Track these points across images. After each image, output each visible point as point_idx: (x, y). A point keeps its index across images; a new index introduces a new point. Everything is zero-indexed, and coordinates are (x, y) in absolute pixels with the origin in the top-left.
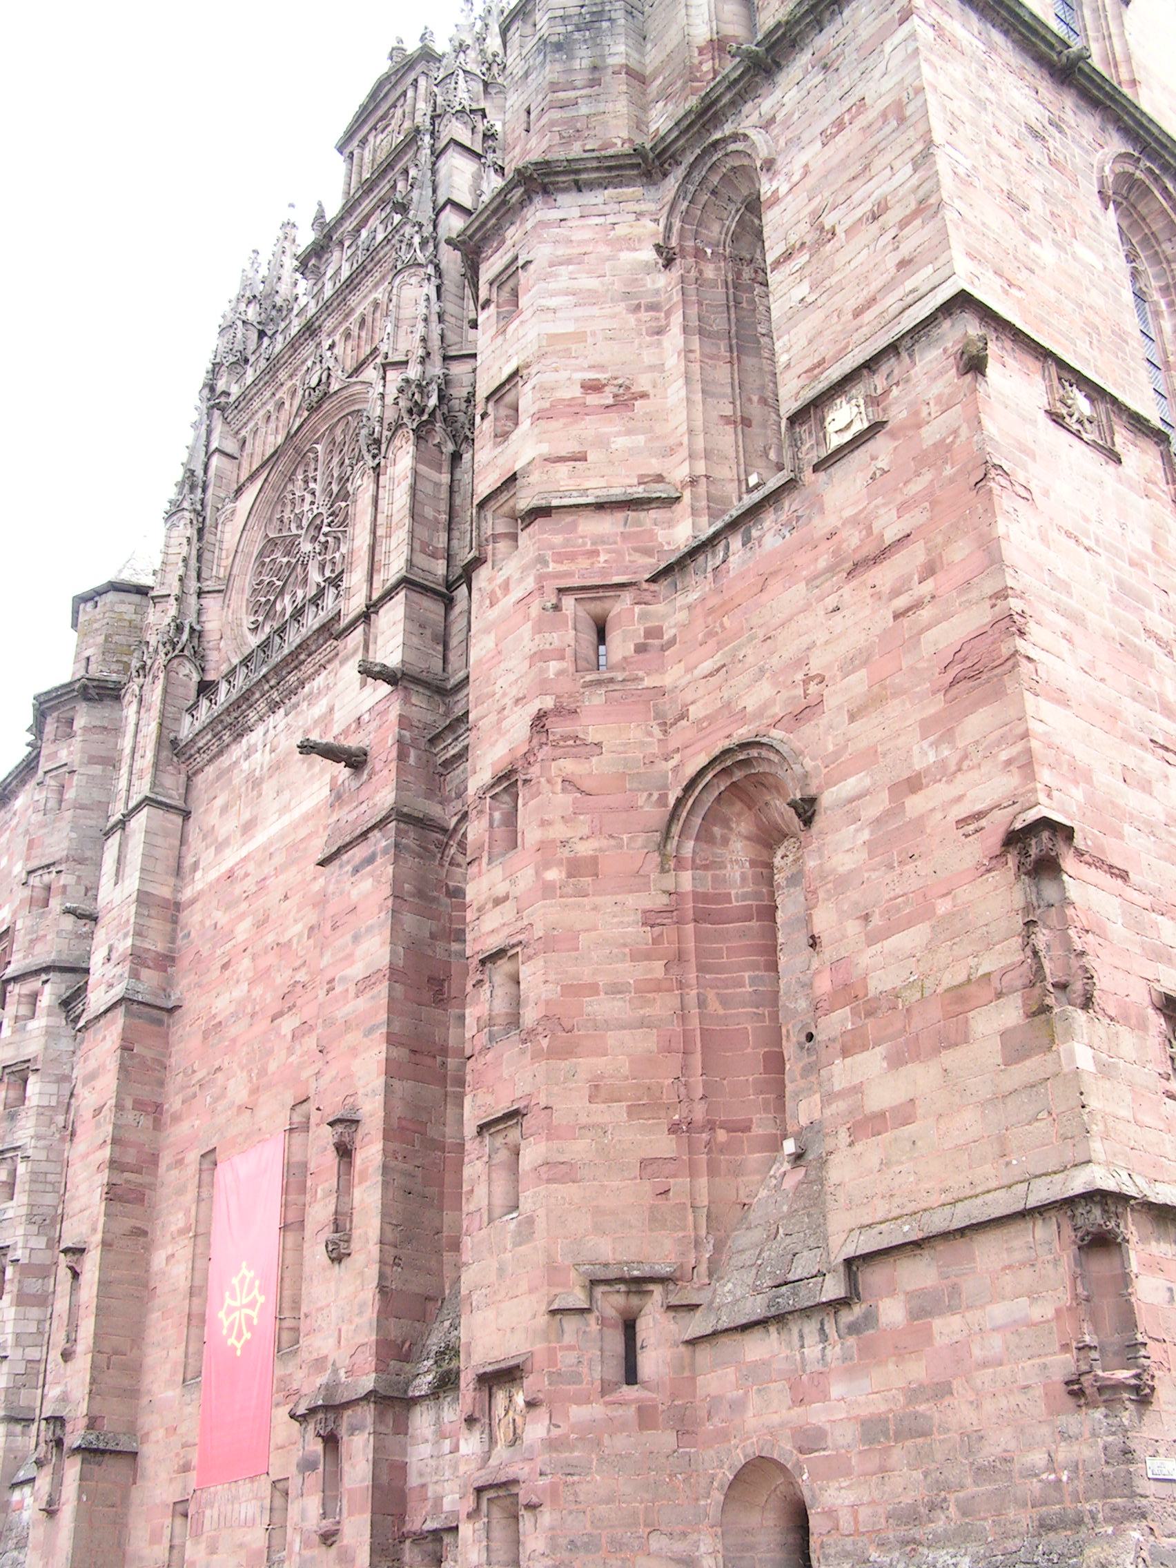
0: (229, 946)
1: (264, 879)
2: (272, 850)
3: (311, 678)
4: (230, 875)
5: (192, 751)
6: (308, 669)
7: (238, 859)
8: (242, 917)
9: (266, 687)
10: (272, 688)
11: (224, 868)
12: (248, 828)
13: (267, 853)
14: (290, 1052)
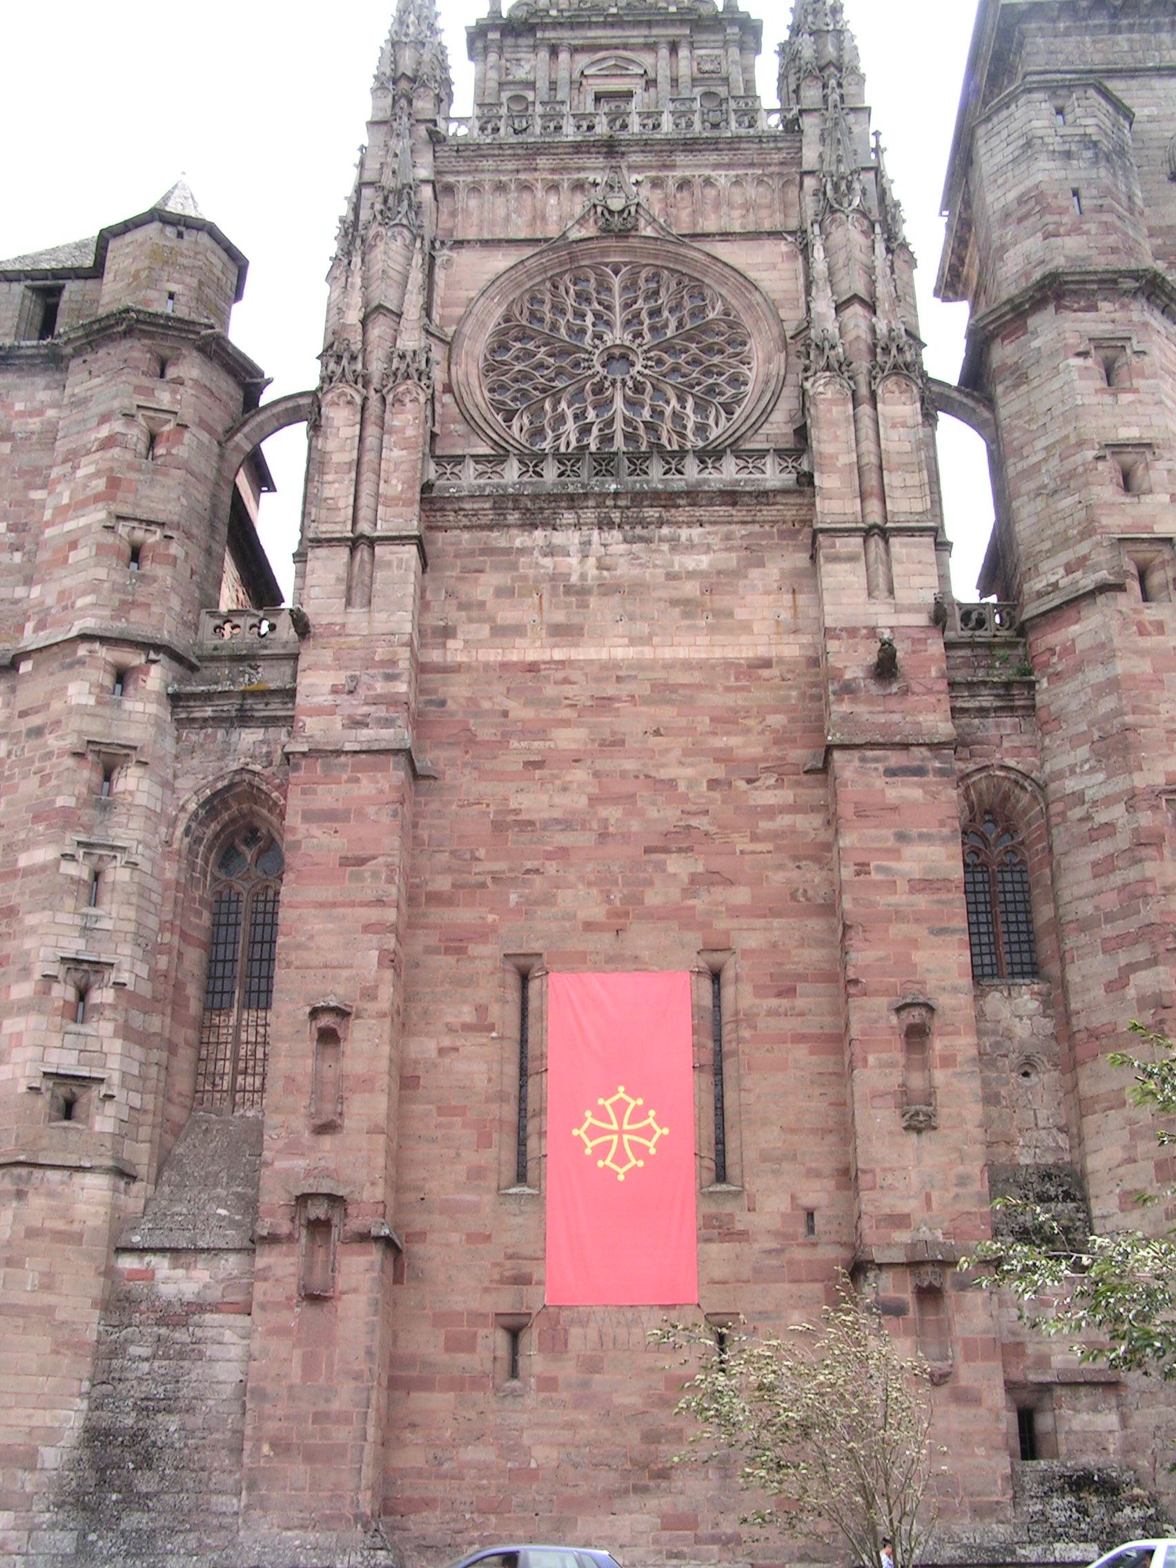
0: (536, 744)
1: (609, 699)
2: (620, 673)
3: (678, 524)
4: (533, 668)
5: (449, 507)
6: (680, 515)
7: (547, 657)
8: (566, 723)
9: (610, 502)
10: (616, 507)
11: (514, 657)
12: (561, 632)
13: (612, 671)
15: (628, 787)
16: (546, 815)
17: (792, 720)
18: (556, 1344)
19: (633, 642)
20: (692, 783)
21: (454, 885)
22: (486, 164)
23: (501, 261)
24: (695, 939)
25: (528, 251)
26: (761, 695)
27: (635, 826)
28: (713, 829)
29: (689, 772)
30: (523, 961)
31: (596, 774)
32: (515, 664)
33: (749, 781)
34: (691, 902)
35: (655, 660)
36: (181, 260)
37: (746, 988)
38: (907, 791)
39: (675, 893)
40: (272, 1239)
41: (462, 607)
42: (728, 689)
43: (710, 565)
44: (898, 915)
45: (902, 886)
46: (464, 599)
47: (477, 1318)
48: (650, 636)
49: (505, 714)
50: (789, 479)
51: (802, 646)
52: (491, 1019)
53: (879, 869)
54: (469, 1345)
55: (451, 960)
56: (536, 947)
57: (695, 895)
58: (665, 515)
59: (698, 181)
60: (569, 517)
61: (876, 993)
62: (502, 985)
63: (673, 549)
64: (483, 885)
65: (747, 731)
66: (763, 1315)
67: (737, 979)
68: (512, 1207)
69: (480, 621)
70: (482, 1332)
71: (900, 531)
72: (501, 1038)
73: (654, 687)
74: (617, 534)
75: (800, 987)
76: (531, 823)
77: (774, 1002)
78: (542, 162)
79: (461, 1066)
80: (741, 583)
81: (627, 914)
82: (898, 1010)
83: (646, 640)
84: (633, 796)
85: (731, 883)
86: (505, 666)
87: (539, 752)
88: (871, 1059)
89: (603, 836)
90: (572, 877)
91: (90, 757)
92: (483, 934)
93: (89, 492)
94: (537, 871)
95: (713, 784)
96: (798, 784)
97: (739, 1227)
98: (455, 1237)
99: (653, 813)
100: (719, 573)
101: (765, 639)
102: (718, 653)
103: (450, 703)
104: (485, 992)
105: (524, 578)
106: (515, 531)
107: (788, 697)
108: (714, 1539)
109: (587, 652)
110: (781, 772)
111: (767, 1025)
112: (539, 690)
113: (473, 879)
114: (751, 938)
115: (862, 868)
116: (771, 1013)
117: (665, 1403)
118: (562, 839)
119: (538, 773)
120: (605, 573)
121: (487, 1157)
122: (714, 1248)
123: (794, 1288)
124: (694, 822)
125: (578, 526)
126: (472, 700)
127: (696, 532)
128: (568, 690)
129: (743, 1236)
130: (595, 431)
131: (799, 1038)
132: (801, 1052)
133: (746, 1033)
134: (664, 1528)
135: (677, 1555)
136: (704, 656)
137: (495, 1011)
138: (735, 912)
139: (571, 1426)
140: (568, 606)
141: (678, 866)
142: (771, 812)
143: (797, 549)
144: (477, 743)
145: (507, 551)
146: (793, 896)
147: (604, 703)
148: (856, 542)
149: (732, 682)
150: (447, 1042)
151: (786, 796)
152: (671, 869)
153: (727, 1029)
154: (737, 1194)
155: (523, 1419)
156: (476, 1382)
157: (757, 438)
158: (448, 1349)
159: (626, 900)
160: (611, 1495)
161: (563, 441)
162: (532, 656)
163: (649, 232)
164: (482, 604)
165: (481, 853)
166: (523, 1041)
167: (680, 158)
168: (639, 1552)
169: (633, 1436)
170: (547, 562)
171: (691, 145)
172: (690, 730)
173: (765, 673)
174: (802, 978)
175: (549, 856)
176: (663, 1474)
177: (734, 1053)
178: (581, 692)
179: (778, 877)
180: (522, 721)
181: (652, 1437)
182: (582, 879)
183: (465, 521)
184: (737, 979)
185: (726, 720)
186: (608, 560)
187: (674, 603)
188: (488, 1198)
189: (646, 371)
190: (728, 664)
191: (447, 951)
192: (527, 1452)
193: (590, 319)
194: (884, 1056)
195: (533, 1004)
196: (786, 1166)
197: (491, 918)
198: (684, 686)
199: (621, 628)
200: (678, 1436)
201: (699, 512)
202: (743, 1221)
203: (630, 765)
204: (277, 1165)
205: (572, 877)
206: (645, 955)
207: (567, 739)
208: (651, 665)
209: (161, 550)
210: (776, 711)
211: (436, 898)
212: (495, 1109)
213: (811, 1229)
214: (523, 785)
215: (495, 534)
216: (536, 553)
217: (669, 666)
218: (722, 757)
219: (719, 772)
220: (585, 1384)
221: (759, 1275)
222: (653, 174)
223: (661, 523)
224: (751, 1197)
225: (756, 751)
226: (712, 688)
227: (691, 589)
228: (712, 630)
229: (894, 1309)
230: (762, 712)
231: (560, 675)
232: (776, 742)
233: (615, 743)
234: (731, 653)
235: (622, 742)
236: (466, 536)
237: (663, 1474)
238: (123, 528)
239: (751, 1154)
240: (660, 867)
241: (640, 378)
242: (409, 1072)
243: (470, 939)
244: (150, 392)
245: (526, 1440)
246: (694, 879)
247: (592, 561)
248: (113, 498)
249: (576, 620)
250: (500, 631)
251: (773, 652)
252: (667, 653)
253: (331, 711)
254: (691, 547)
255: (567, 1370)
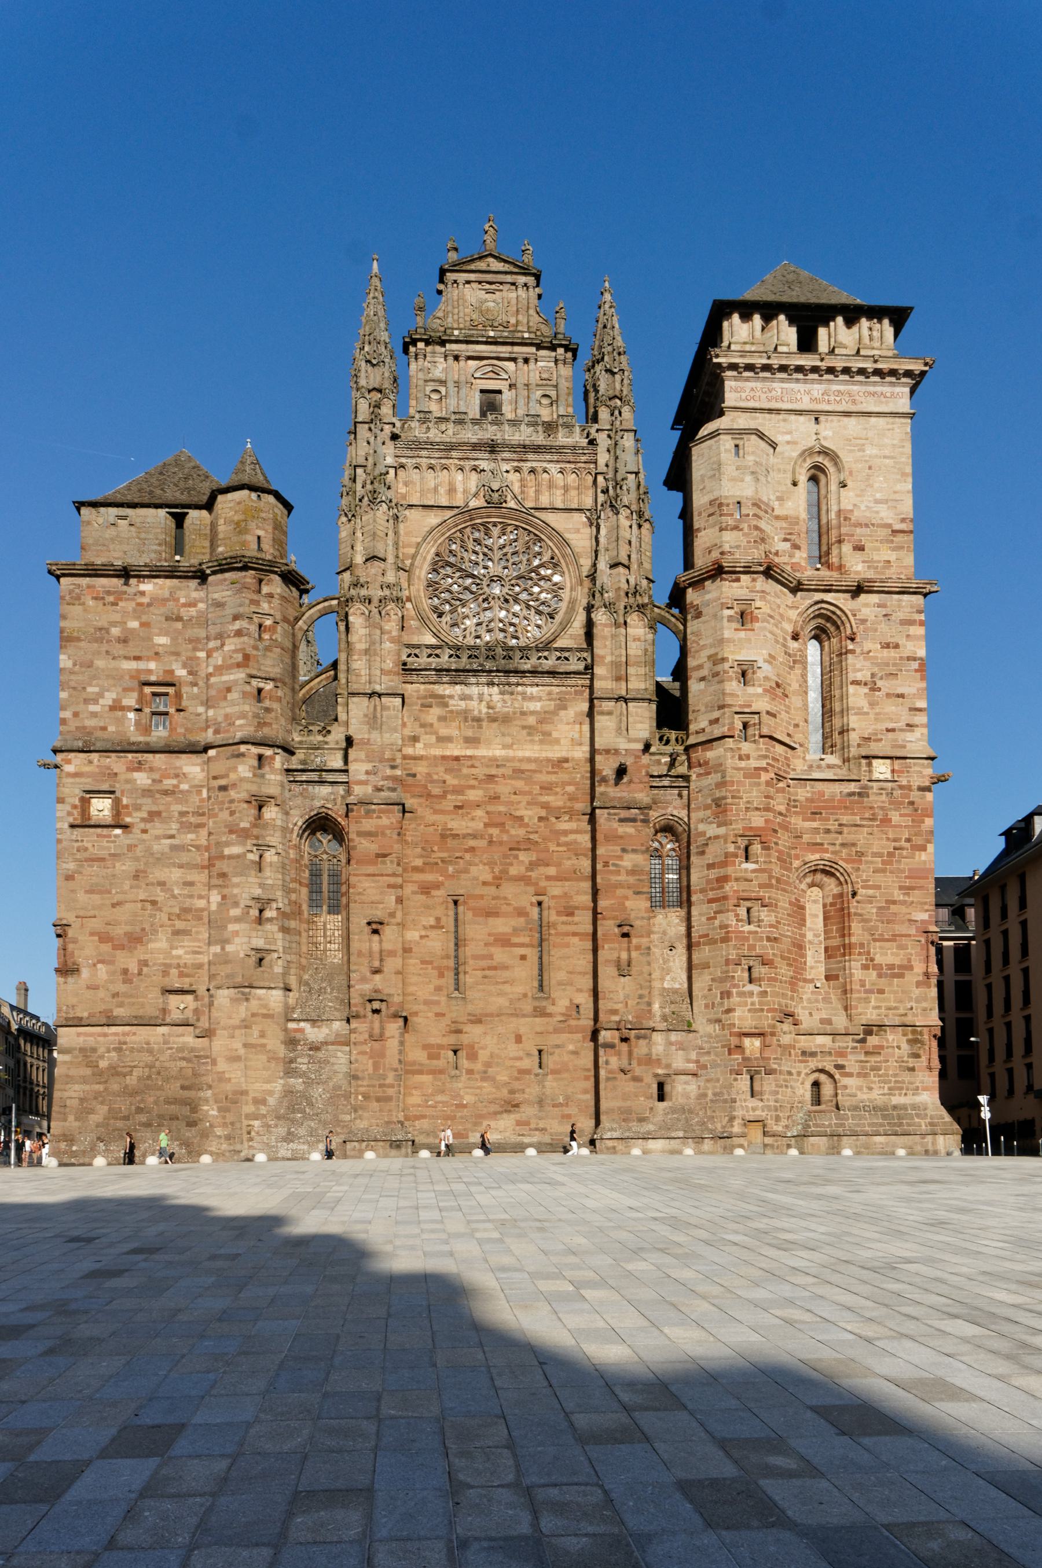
0: (460, 797)
4: (457, 759)
7: (463, 754)
8: (473, 787)
11: (448, 753)
12: (472, 741)
14: (528, 869)
15: (500, 820)
16: (464, 832)
17: (577, 789)
18: (473, 1056)
19: (505, 747)
20: (531, 818)
21: (424, 863)
22: (424, 453)
23: (433, 519)
24: (531, 890)
25: (449, 513)
26: (563, 776)
27: (505, 838)
28: (540, 840)
29: (529, 813)
30: (455, 898)
31: (487, 813)
32: (448, 757)
33: (557, 818)
34: (529, 874)
35: (514, 757)
36: (263, 515)
37: (553, 912)
38: (629, 829)
39: (523, 869)
40: (357, 1016)
41: (422, 726)
42: (548, 773)
43: (542, 707)
44: (620, 885)
45: (623, 871)
46: (422, 721)
47: (441, 1047)
48: (512, 744)
49: (444, 782)
50: (581, 666)
51: (583, 752)
52: (442, 924)
53: (614, 865)
54: (437, 1057)
55: (423, 897)
56: (461, 892)
57: (532, 870)
58: (521, 681)
59: (540, 470)
60: (473, 680)
61: (609, 919)
62: (447, 909)
63: (524, 699)
64: (437, 864)
65: (556, 794)
66: (557, 1046)
67: (549, 908)
68: (454, 1002)
69: (431, 733)
70: (442, 1052)
71: (634, 699)
72: (447, 932)
73: (514, 771)
74: (496, 688)
75: (576, 912)
76: (458, 835)
77: (564, 918)
78: (454, 454)
79: (430, 943)
80: (556, 718)
81: (501, 878)
82: (620, 926)
83: (509, 747)
84: (503, 824)
85: (548, 865)
86: (444, 758)
87: (461, 801)
88: (606, 946)
89: (491, 842)
90: (477, 860)
91: (254, 803)
92: (437, 886)
93: (233, 661)
94: (461, 858)
95: (541, 819)
96: (579, 820)
97: (548, 1011)
98: (430, 1014)
99: (513, 832)
100: (545, 712)
101: (566, 748)
102: (544, 755)
103: (418, 776)
104: (439, 912)
105: (452, 712)
106: (447, 686)
107: (575, 778)
108: (537, 1129)
109: (482, 752)
110: (572, 813)
111: (562, 928)
112: (460, 770)
113: (432, 860)
114: (556, 890)
115: (606, 864)
116: (563, 923)
117: (517, 1079)
118: (472, 843)
119: (460, 811)
120: (491, 711)
121: (442, 982)
122: (538, 1020)
123: (570, 1035)
124: (532, 837)
125: (477, 684)
126: (429, 774)
127: (535, 689)
128: (473, 771)
129: (550, 1015)
130: (484, 625)
131: (575, 934)
132: (575, 940)
133: (552, 932)
134: (517, 1125)
135: (523, 1135)
136: (537, 755)
137: (444, 920)
138: (549, 878)
139: (478, 1088)
140: (473, 727)
141: (523, 856)
142: (566, 833)
143: (583, 701)
144: (433, 796)
145: (442, 697)
146: (575, 872)
147: (491, 778)
148: (612, 704)
149: (550, 769)
150: (423, 933)
151: (573, 825)
152: (521, 858)
153: (544, 929)
154: (547, 998)
155: (460, 1085)
156: (441, 1072)
157: (566, 636)
158: (429, 1058)
159: (501, 872)
160: (496, 1113)
161: (467, 632)
162: (456, 753)
163: (512, 504)
164: (431, 725)
165: (436, 848)
166: (456, 932)
167: (530, 456)
168: (507, 1134)
169: (505, 1091)
170: (463, 704)
171: (537, 449)
172: (530, 793)
173: (566, 765)
174: (577, 908)
175: (467, 851)
176: (517, 1106)
177: (548, 940)
178: (480, 772)
179: (568, 864)
180: (453, 786)
181: (512, 1092)
182: (481, 862)
183: (422, 680)
184: (549, 908)
185: (546, 788)
186: (491, 704)
187: (524, 727)
188: (443, 999)
189: (510, 593)
190: (548, 760)
191: (422, 893)
192: (462, 1098)
193: (481, 556)
194: (612, 945)
195: (461, 917)
196: (568, 987)
197: (441, 879)
198: (528, 771)
199: (498, 740)
200: (523, 1091)
201: (536, 680)
202: (550, 1009)
203: (502, 808)
204: (357, 987)
205: (477, 860)
206: (510, 896)
207: (474, 795)
208: (512, 759)
209: (273, 694)
210: (570, 784)
211: (416, 869)
212: (445, 962)
213: (578, 1012)
214: (454, 816)
215: (436, 687)
216: (456, 698)
217: (521, 760)
218: (545, 806)
219: (543, 813)
220: (485, 1072)
221: (556, 1031)
222: (516, 464)
223: (518, 684)
224: (553, 1000)
225: (560, 804)
226: (541, 772)
227: (531, 720)
228: (541, 742)
229: (612, 1046)
230: (564, 784)
231: (470, 763)
232: (570, 800)
233: (495, 798)
234: (550, 755)
235: (499, 798)
236: (422, 687)
237: (517, 1106)
238: (255, 683)
239: (553, 982)
240: (516, 857)
241: (508, 597)
242: (407, 946)
243: (433, 888)
244: (257, 603)
245: (462, 1093)
246: (531, 863)
247: (484, 703)
248: (247, 666)
249: (477, 735)
250: (442, 740)
251: (570, 755)
252: (520, 754)
253: (365, 783)
254: (532, 698)
255: (478, 1066)
